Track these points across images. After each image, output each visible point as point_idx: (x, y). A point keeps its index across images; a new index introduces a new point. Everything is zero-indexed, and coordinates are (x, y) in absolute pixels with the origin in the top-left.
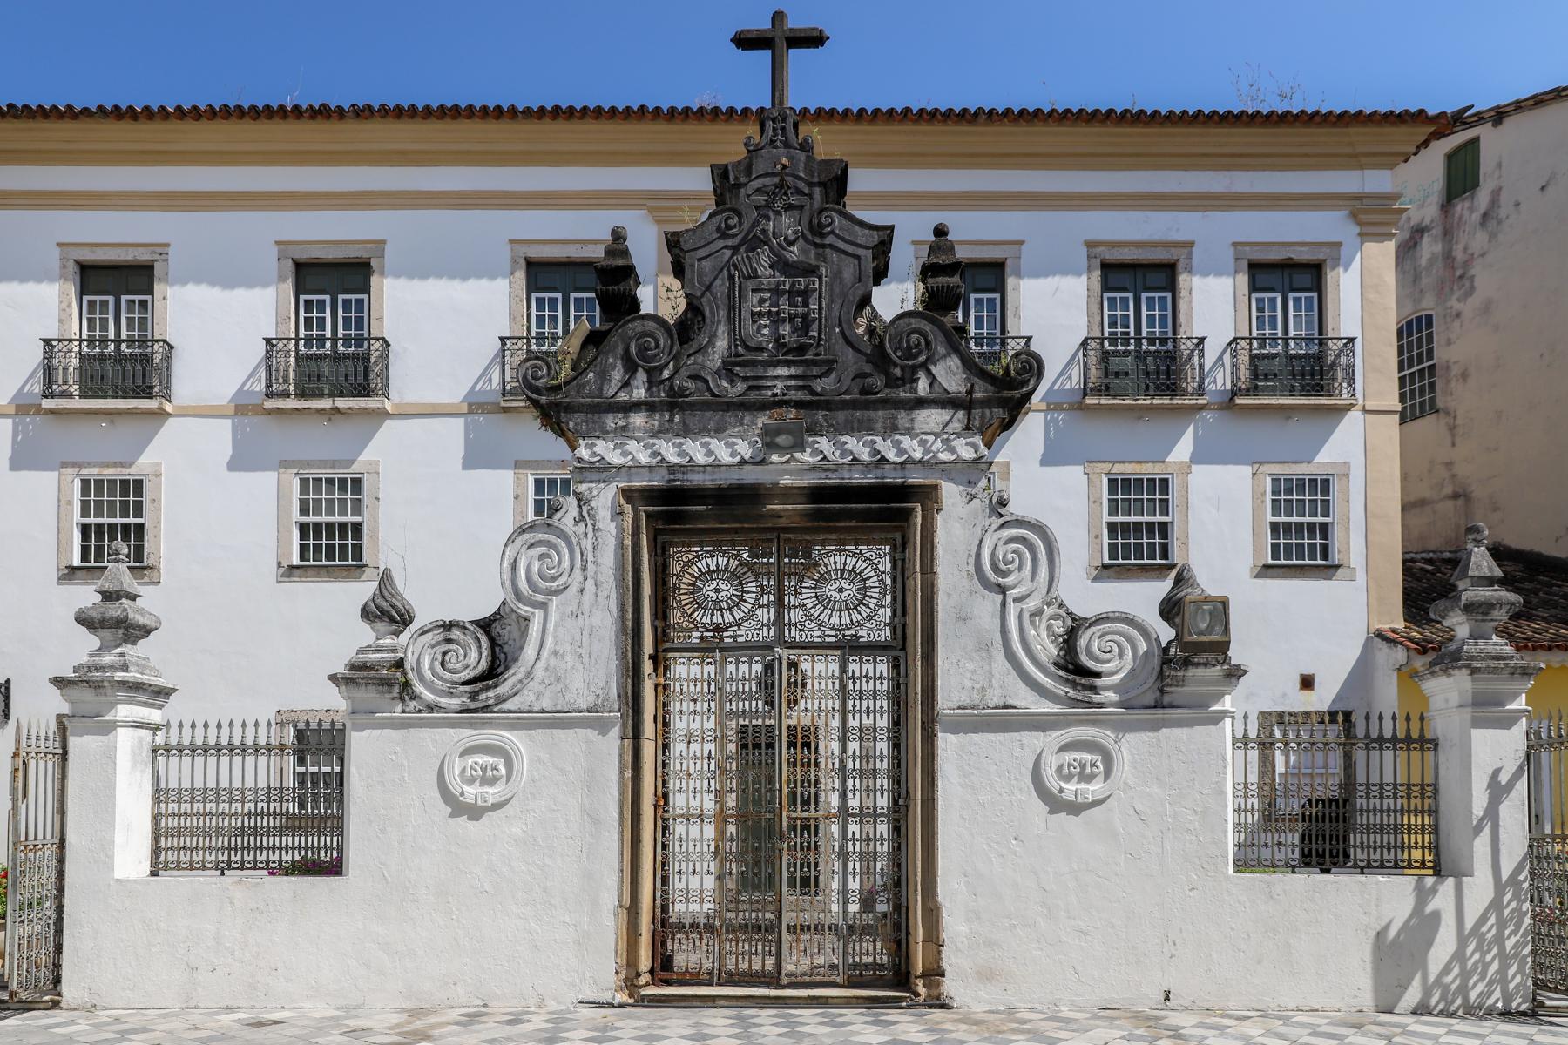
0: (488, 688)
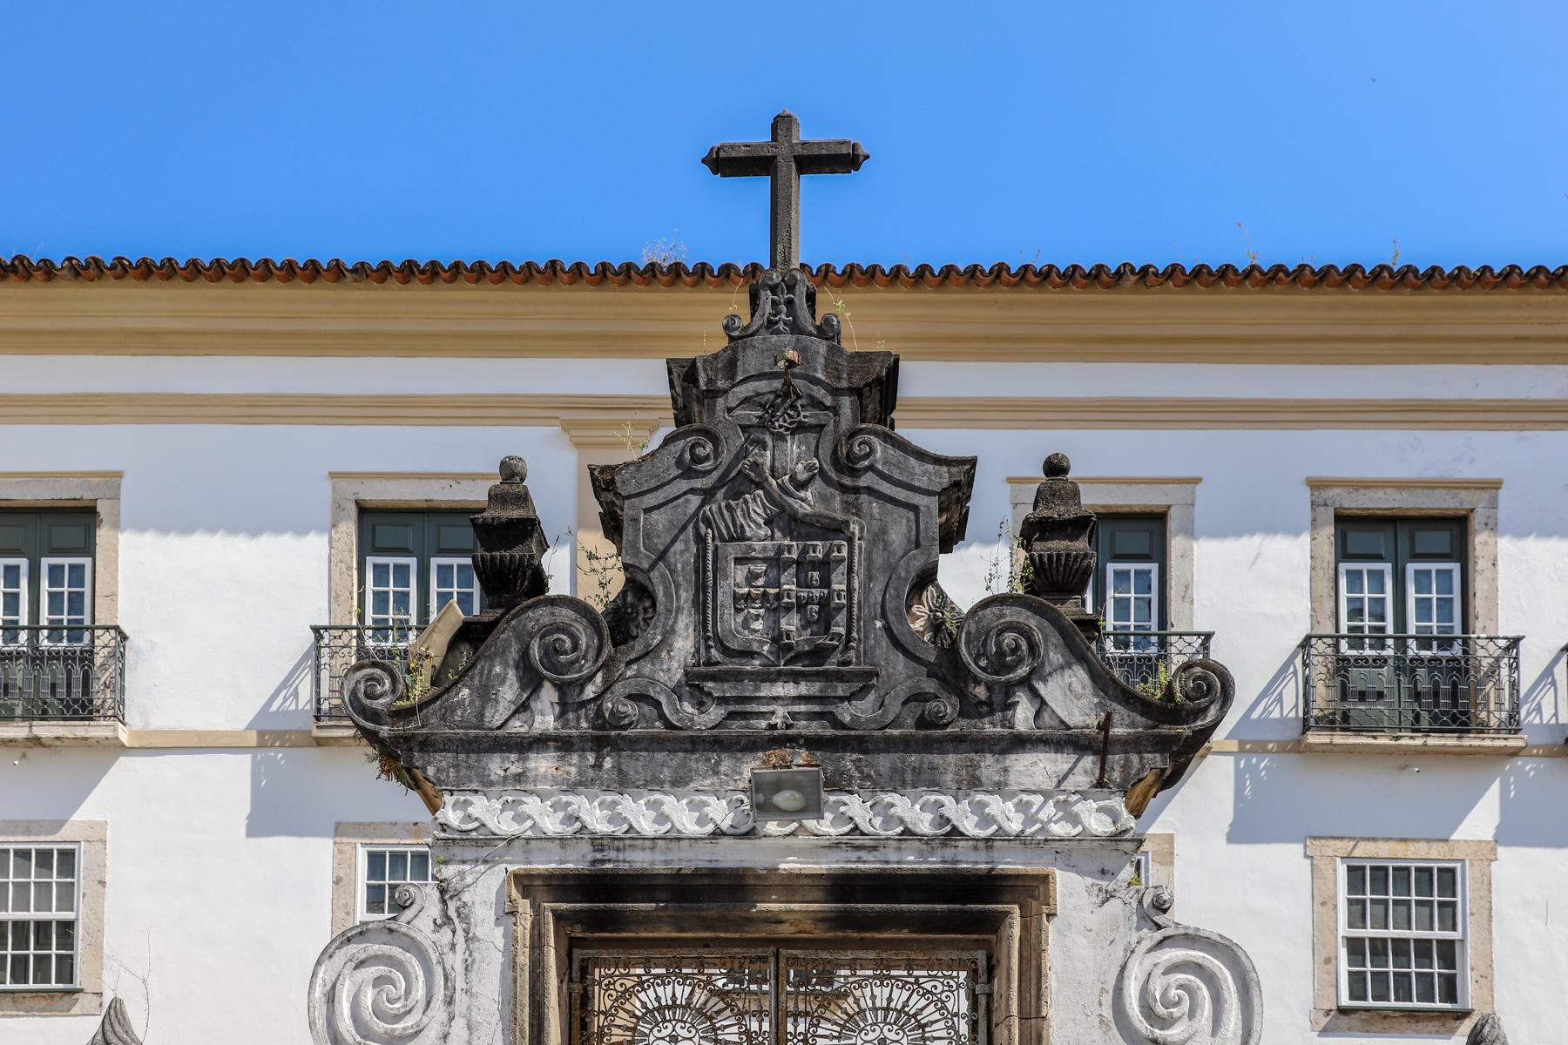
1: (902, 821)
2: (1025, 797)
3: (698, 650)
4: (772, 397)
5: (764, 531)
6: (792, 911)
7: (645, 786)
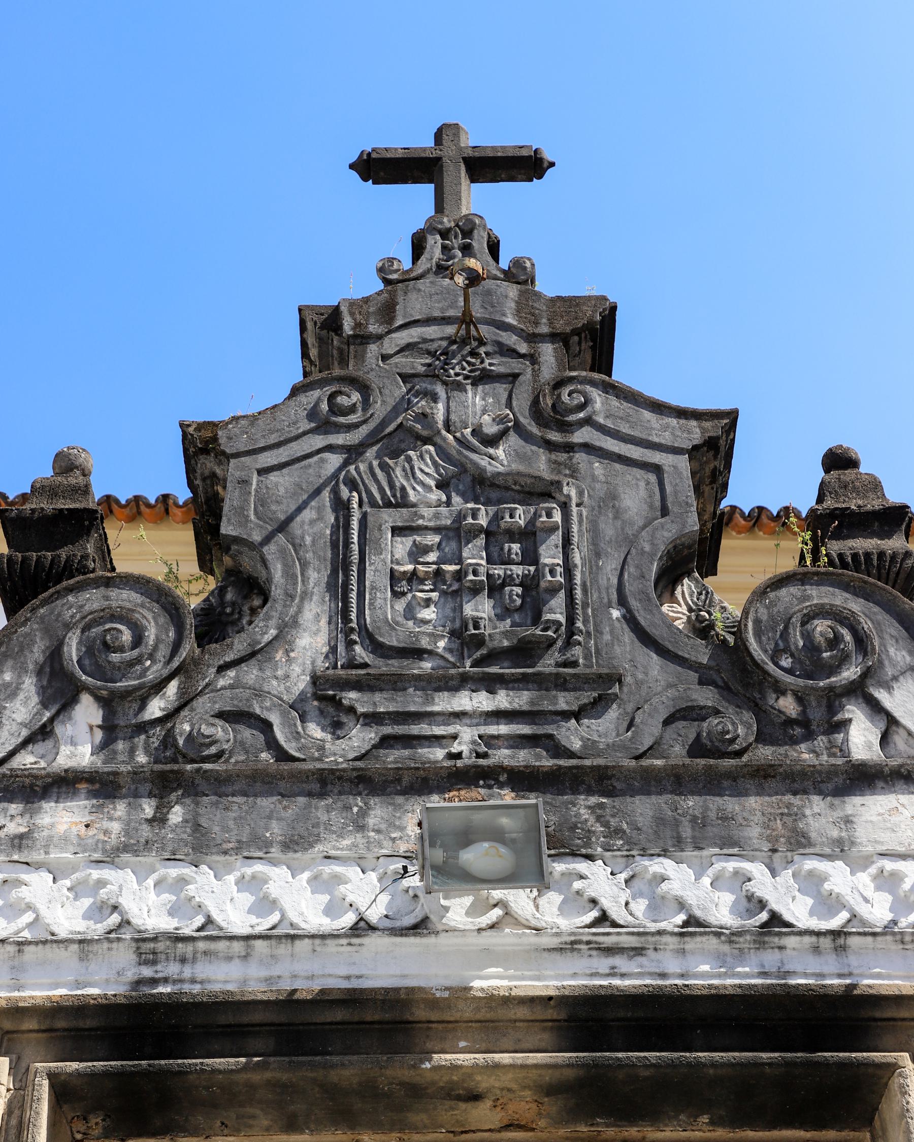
1: (681, 905)
2: (889, 865)
3: (333, 650)
4: (444, 344)
5: (437, 495)
6: (497, 1066)
7: (238, 850)
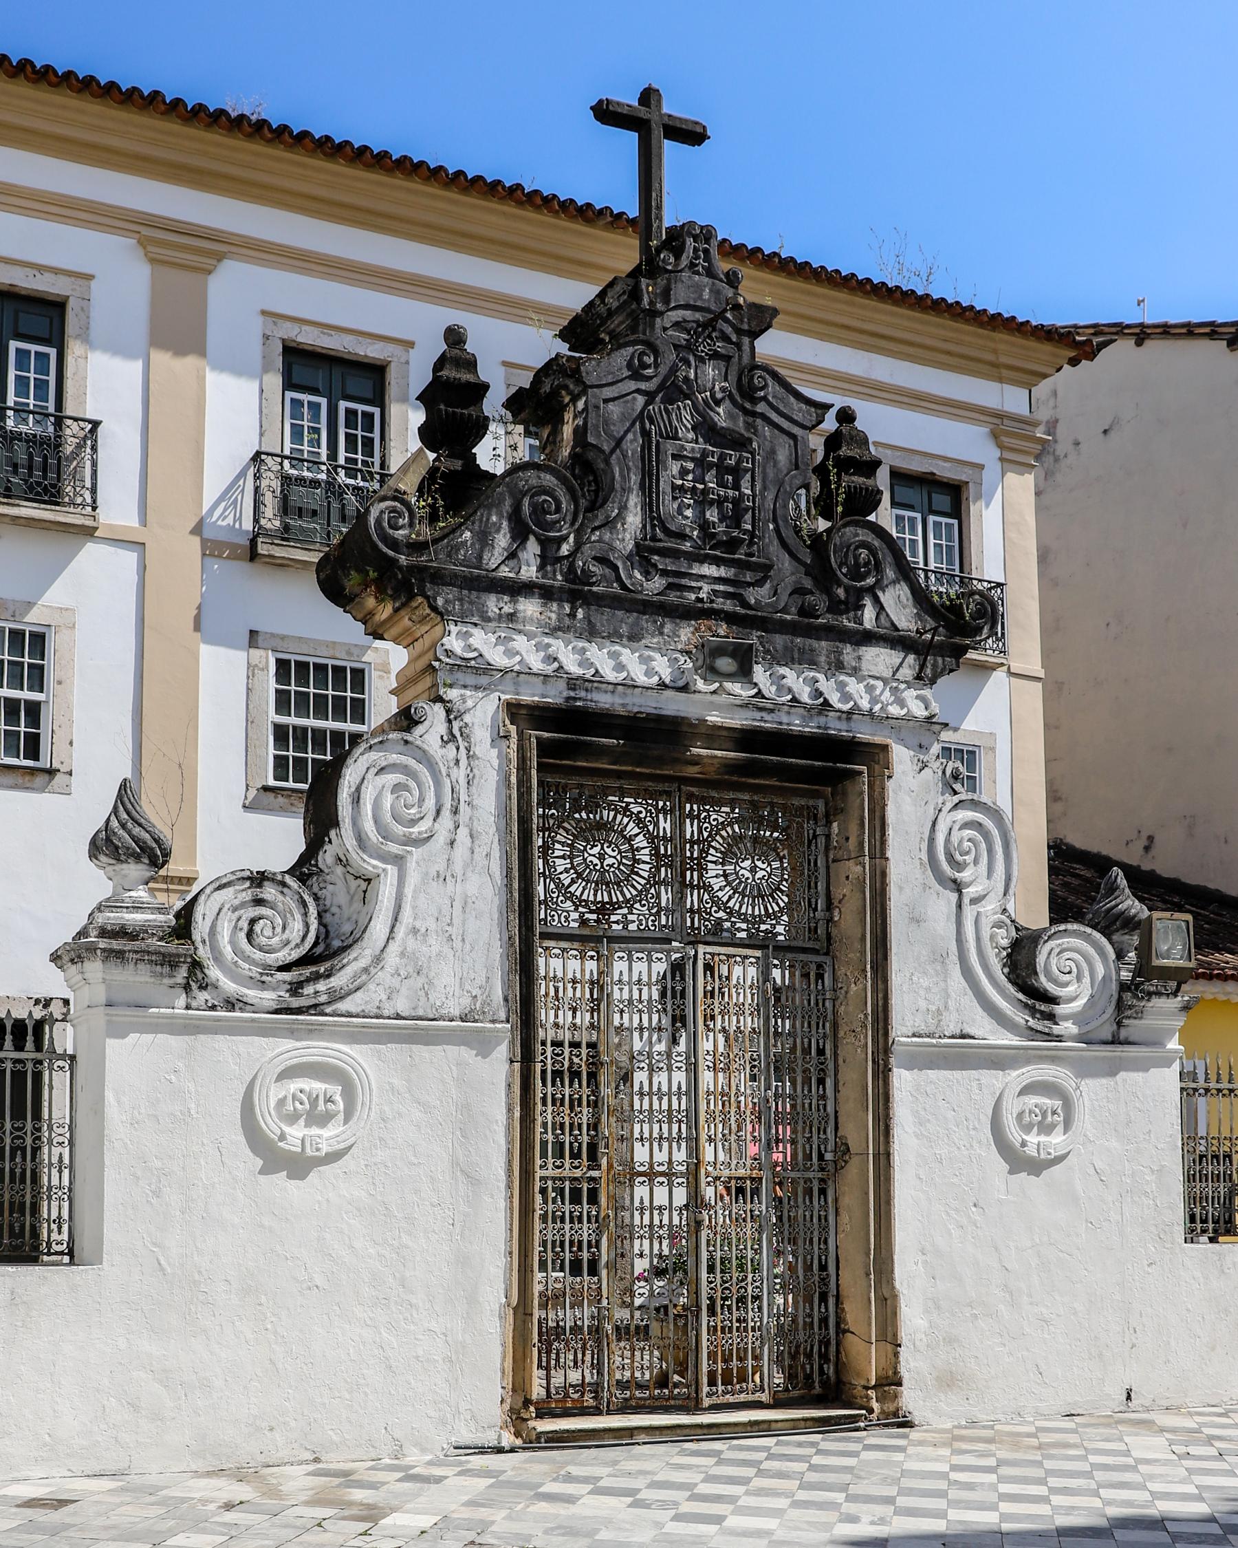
0: (316, 977)
1: (790, 690)
2: (872, 682)
3: (644, 526)
5: (691, 435)
6: (716, 757)
7: (609, 637)
